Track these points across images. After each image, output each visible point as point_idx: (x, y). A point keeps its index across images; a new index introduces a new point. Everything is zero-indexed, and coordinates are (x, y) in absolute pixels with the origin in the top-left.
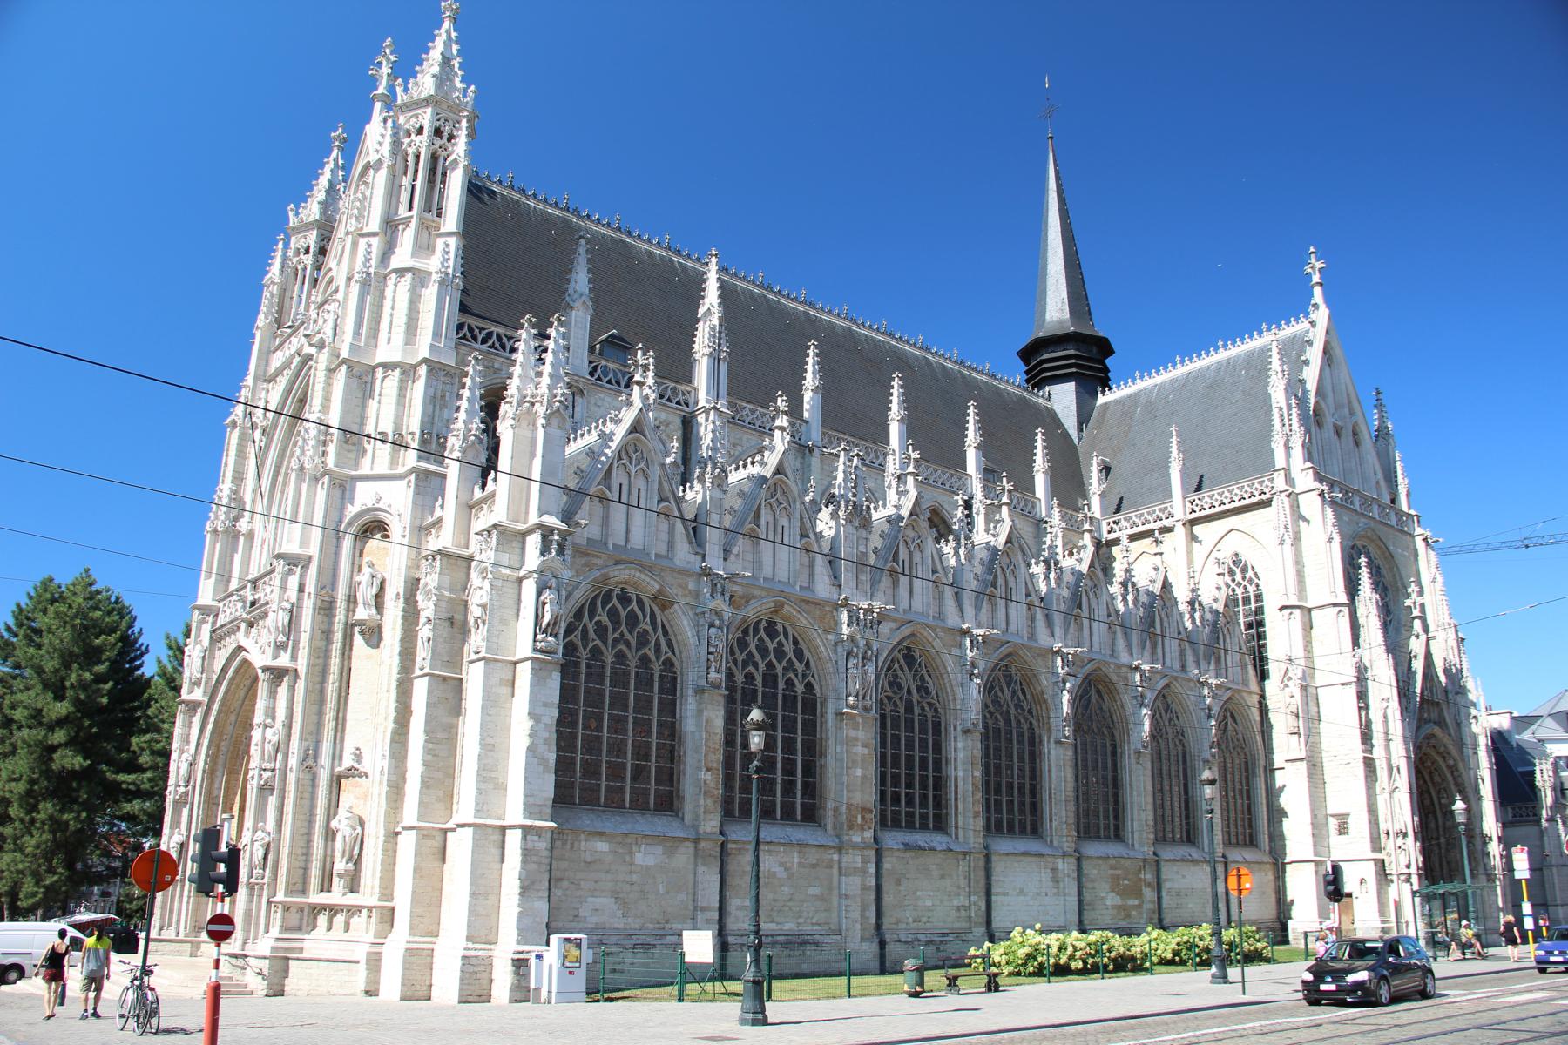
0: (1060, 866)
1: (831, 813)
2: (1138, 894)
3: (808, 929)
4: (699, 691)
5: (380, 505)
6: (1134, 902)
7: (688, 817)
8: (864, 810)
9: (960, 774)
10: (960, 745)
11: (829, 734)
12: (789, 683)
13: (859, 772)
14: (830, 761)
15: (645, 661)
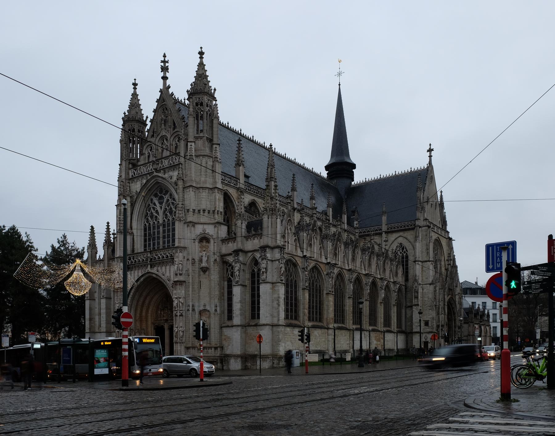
0: (366, 333)
1: (325, 320)
2: (380, 341)
3: (322, 349)
4: (304, 289)
5: (206, 232)
6: (379, 343)
7: (301, 321)
8: (332, 319)
9: (348, 309)
10: (348, 301)
11: (325, 299)
12: (316, 285)
13: (331, 309)
14: (325, 306)
15: (291, 280)
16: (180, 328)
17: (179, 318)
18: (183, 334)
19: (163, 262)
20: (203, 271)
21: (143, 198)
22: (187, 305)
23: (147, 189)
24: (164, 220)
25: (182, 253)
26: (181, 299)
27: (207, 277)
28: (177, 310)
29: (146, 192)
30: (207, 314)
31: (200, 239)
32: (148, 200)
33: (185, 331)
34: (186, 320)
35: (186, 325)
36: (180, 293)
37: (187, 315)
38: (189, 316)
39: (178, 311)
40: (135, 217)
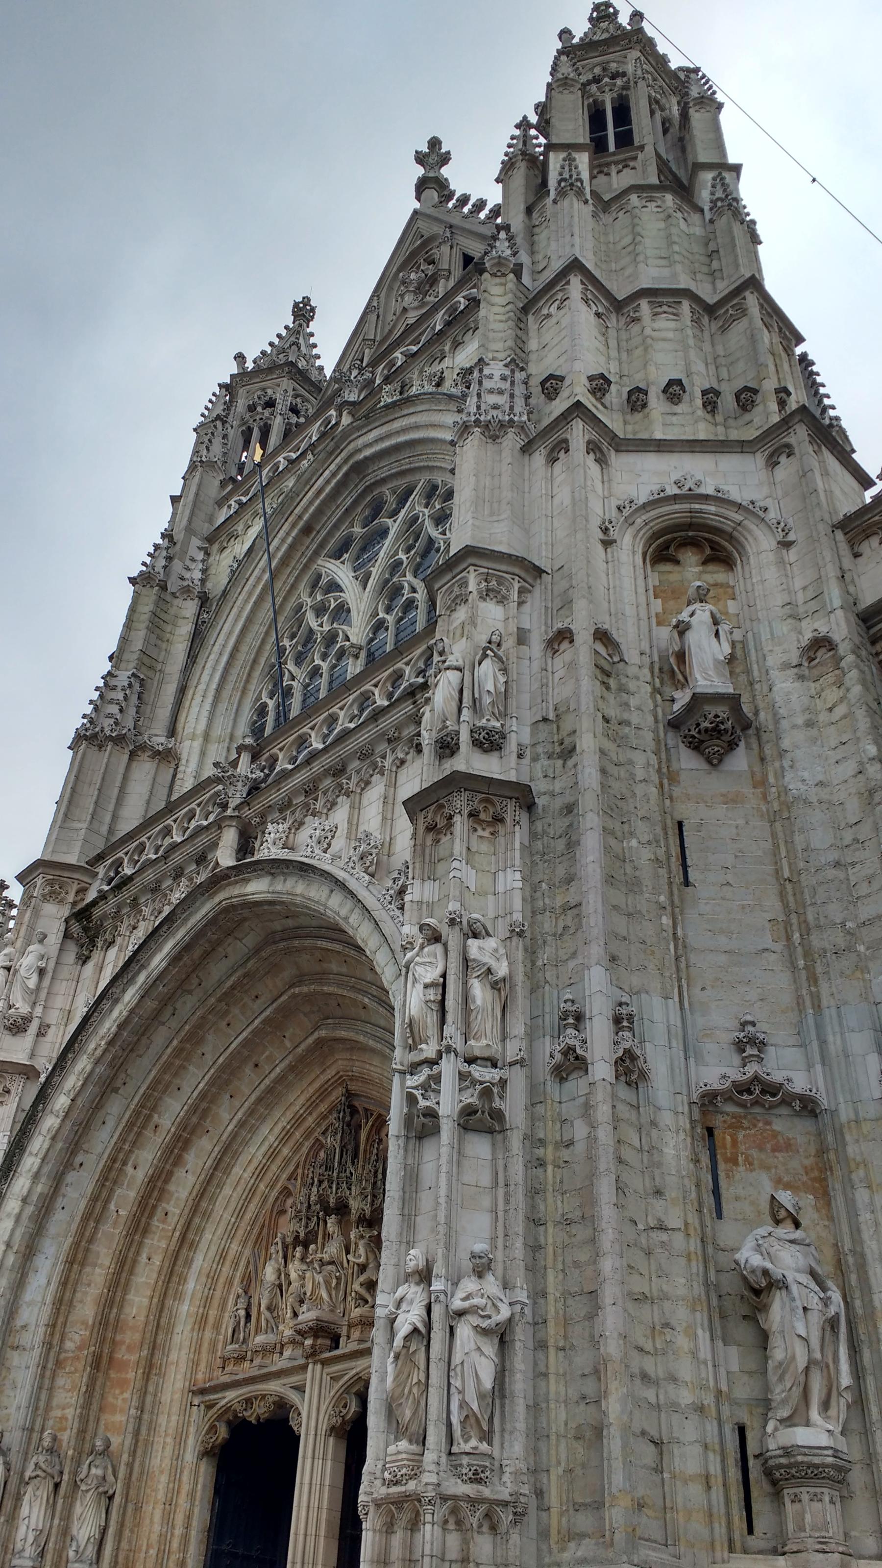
16: (469, 1285)
17: (460, 1154)
18: (502, 1374)
19: (339, 771)
20: (696, 746)
21: (267, 576)
22: (551, 1019)
23: (293, 526)
24: (380, 626)
25: (502, 600)
26: (491, 943)
27: (747, 790)
28: (432, 1063)
29: (290, 540)
30: (788, 1146)
31: (655, 536)
32: (293, 587)
33: (521, 1336)
34: (534, 1192)
35: (535, 1248)
36: (481, 893)
37: (550, 1131)
38: (580, 1130)
39: (448, 1068)
40: (205, 677)
